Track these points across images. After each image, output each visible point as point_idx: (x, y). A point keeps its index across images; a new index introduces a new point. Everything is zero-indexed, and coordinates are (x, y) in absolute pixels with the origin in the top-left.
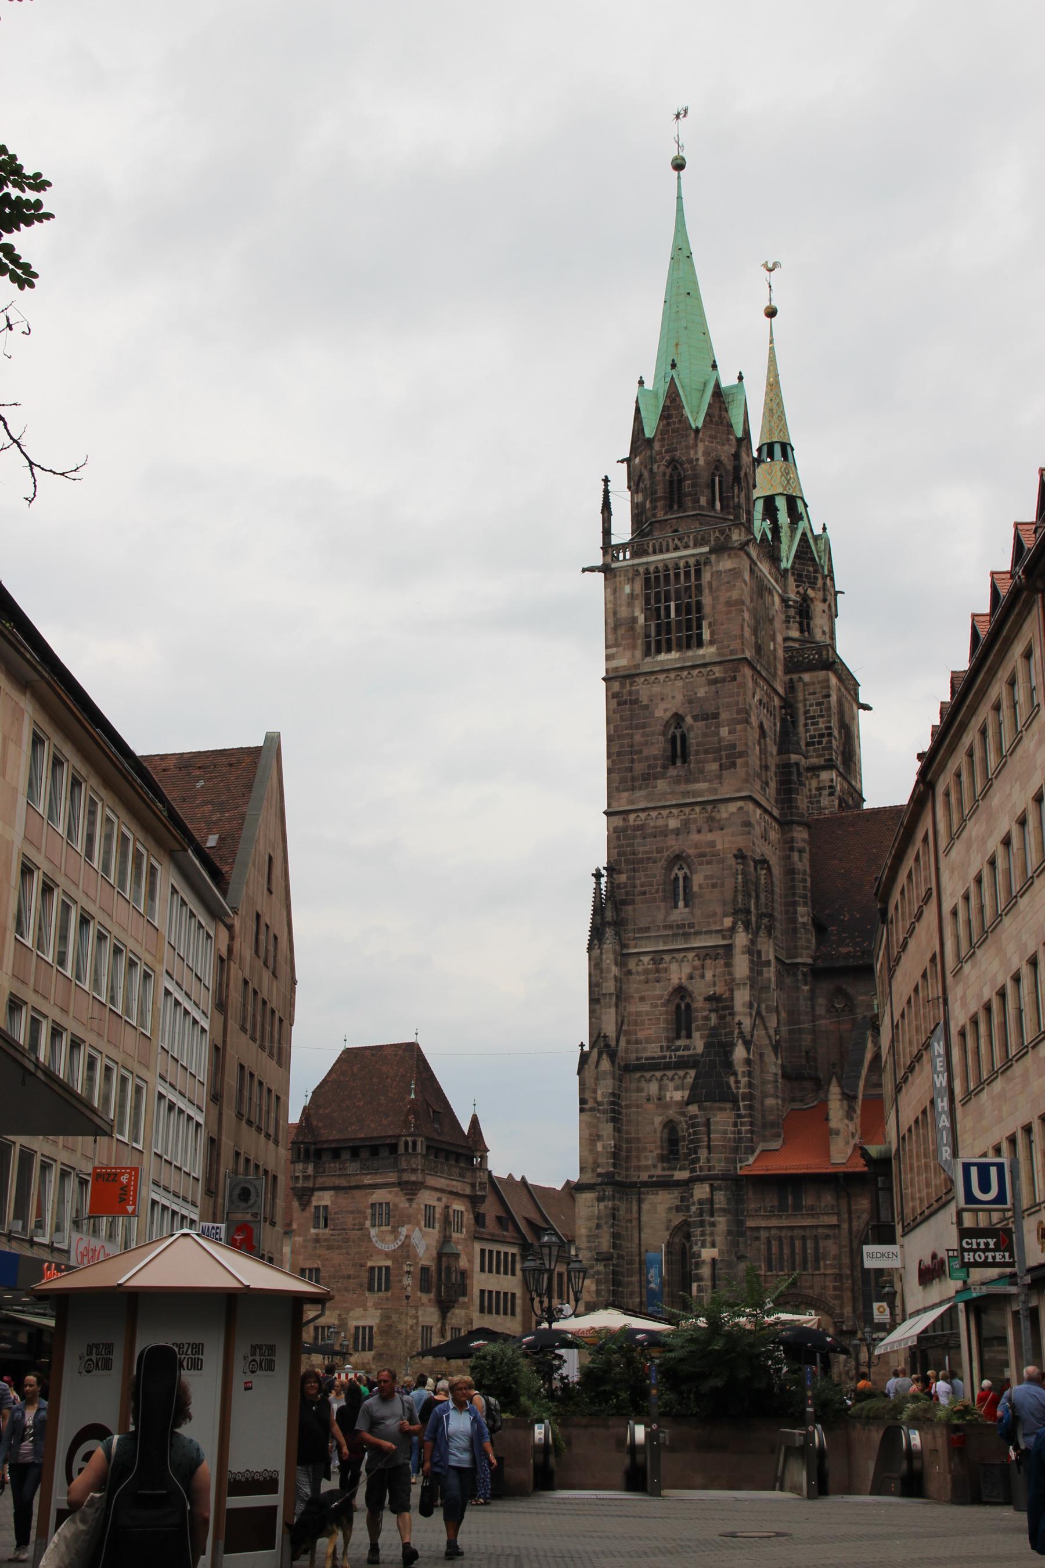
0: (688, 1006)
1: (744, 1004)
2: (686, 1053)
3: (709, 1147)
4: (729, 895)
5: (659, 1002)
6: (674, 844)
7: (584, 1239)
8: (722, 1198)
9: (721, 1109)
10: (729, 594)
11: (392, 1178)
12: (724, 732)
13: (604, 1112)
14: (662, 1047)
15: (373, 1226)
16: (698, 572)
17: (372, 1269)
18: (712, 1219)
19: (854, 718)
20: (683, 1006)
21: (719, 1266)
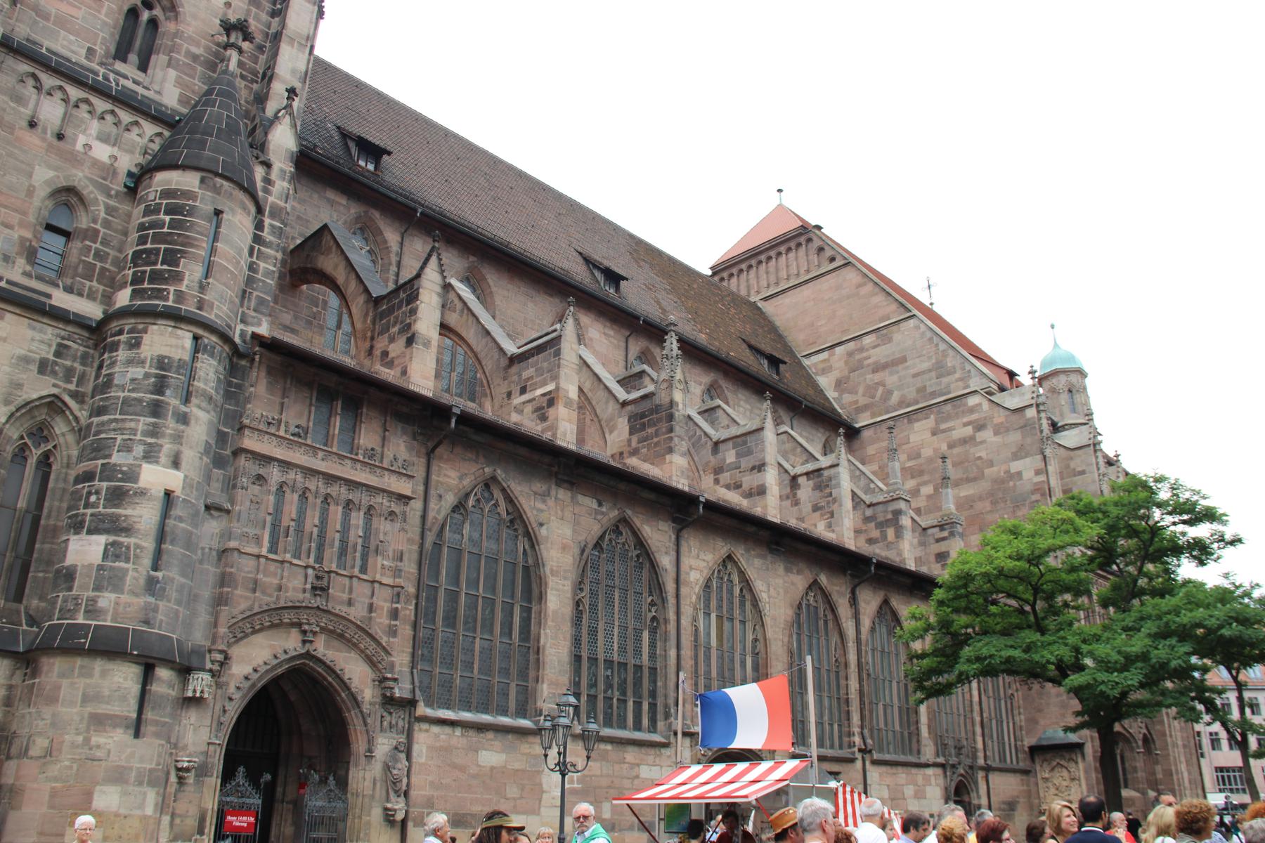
0: (153, 23)
1: (294, 71)
2: (140, 90)
8: (212, 376)
9: (244, 208)
14: (91, 52)
18: (183, 408)
20: (145, 15)
21: (177, 511)
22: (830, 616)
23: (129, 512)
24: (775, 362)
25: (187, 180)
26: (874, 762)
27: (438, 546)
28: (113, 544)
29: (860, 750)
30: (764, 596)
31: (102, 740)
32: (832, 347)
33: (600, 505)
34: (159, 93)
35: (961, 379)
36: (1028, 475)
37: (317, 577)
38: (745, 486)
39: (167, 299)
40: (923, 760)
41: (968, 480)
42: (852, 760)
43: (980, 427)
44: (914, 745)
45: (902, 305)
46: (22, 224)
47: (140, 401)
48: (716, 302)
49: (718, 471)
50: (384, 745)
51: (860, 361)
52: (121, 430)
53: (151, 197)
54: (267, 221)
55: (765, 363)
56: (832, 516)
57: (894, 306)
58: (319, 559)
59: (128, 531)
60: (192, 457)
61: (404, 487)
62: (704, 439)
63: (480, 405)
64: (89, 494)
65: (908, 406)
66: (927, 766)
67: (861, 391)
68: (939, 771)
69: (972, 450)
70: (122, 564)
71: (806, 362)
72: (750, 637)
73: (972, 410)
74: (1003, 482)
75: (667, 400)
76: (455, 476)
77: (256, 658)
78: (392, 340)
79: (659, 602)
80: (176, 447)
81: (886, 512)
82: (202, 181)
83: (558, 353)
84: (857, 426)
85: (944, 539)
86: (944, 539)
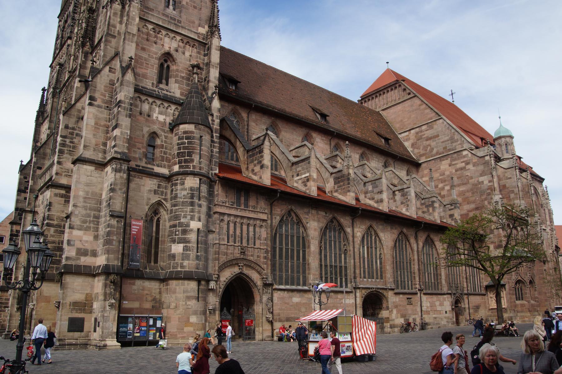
0: (168, 67)
1: (215, 78)
2: (168, 93)
5: (155, 56)
14: (153, 84)
18: (200, 202)
20: (166, 66)
22: (407, 243)
23: (188, 236)
24: (387, 140)
25: (190, 127)
26: (424, 294)
27: (276, 234)
28: (185, 246)
29: (419, 290)
30: (383, 238)
31: (190, 303)
32: (410, 130)
33: (326, 214)
34: (174, 93)
35: (460, 144)
36: (486, 182)
37: (242, 249)
38: (376, 199)
39: (190, 168)
40: (443, 292)
41: (463, 184)
42: (416, 294)
43: (467, 163)
44: (440, 287)
45: (437, 113)
46: (143, 147)
47: (187, 202)
48: (363, 115)
49: (366, 193)
50: (265, 298)
51: (421, 136)
52: (183, 211)
53: (180, 134)
54: (214, 134)
55: (383, 140)
56: (408, 206)
57: (434, 114)
58: (242, 243)
59: (189, 242)
60: (203, 217)
61: (264, 217)
62: (360, 181)
63: (279, 172)
64: (176, 231)
65: (440, 154)
66: (444, 294)
67: (421, 148)
68: (449, 296)
69: (464, 173)
70: (189, 252)
71: (400, 136)
72: (378, 253)
73: (464, 157)
74: (476, 185)
75: (347, 173)
76: (279, 211)
77: (227, 275)
78: (255, 166)
79: (347, 244)
80: (199, 215)
81: (429, 201)
82: (195, 127)
83: (309, 163)
84: (420, 162)
85: (452, 209)
86: (452, 209)
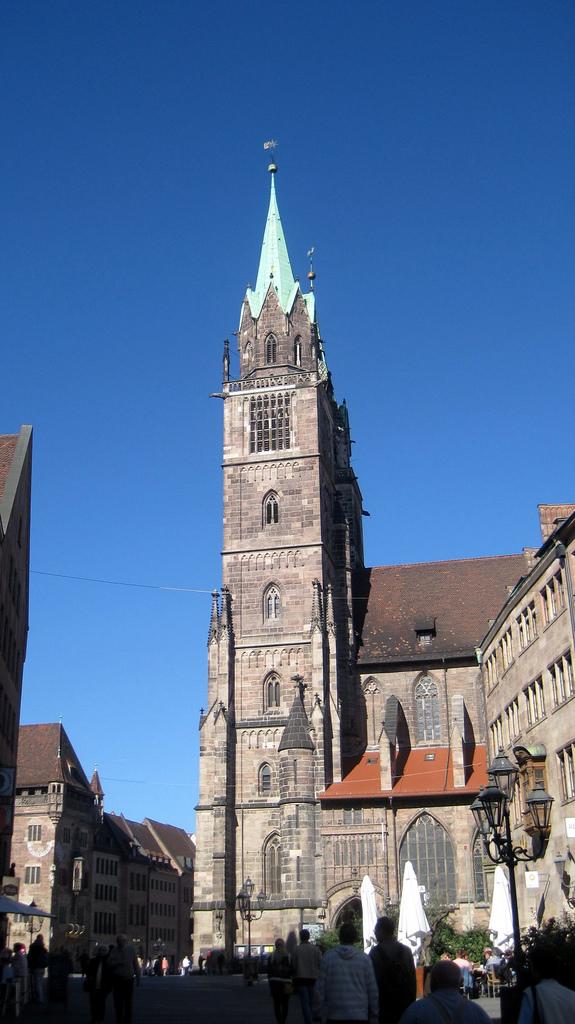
0: (277, 684)
3: (295, 780)
4: (308, 609)
6: (269, 575)
7: (203, 844)
10: (308, 415)
11: (44, 809)
12: (305, 502)
13: (220, 755)
15: (30, 840)
16: (287, 402)
17: (28, 868)
19: (360, 518)
59: (289, 872)
